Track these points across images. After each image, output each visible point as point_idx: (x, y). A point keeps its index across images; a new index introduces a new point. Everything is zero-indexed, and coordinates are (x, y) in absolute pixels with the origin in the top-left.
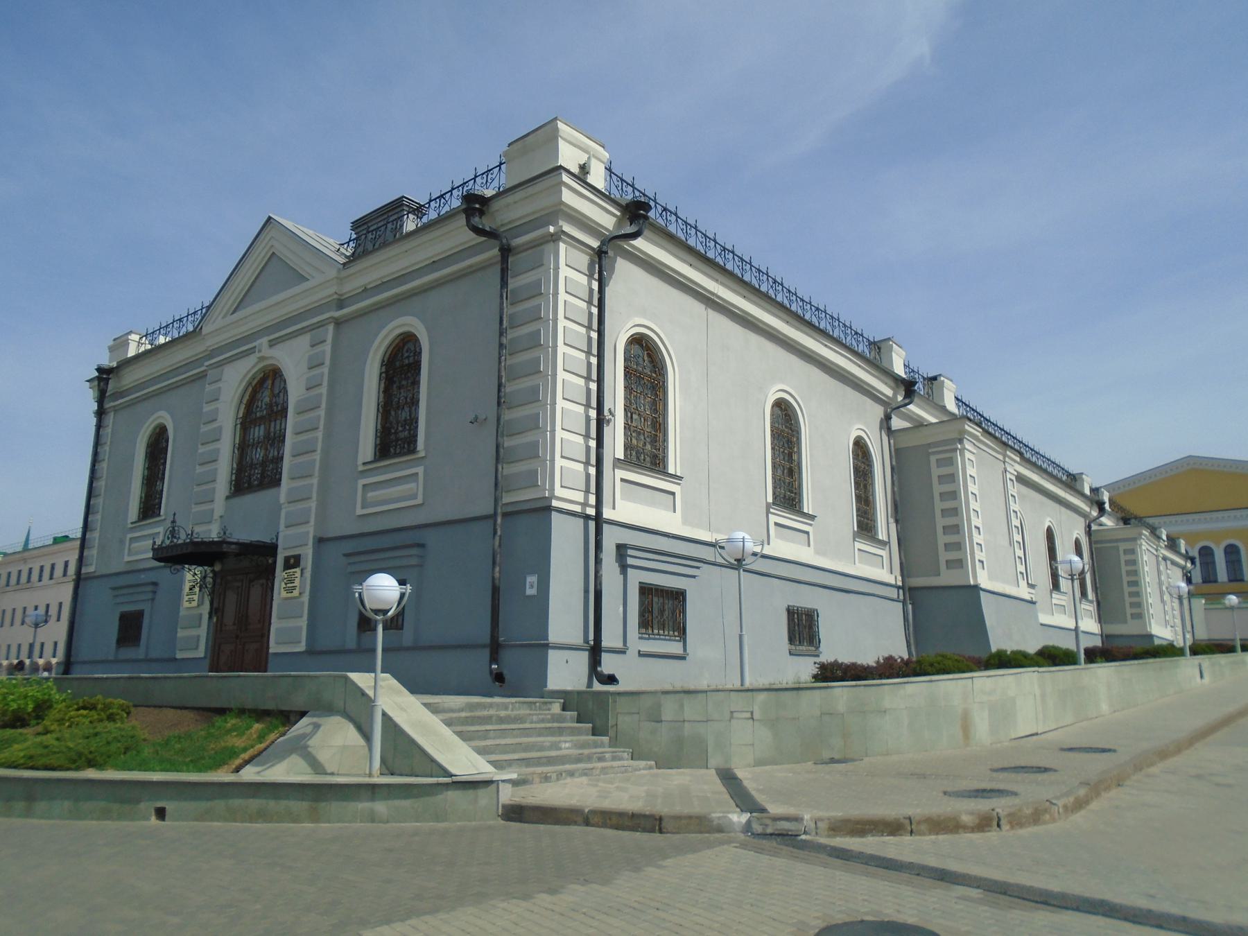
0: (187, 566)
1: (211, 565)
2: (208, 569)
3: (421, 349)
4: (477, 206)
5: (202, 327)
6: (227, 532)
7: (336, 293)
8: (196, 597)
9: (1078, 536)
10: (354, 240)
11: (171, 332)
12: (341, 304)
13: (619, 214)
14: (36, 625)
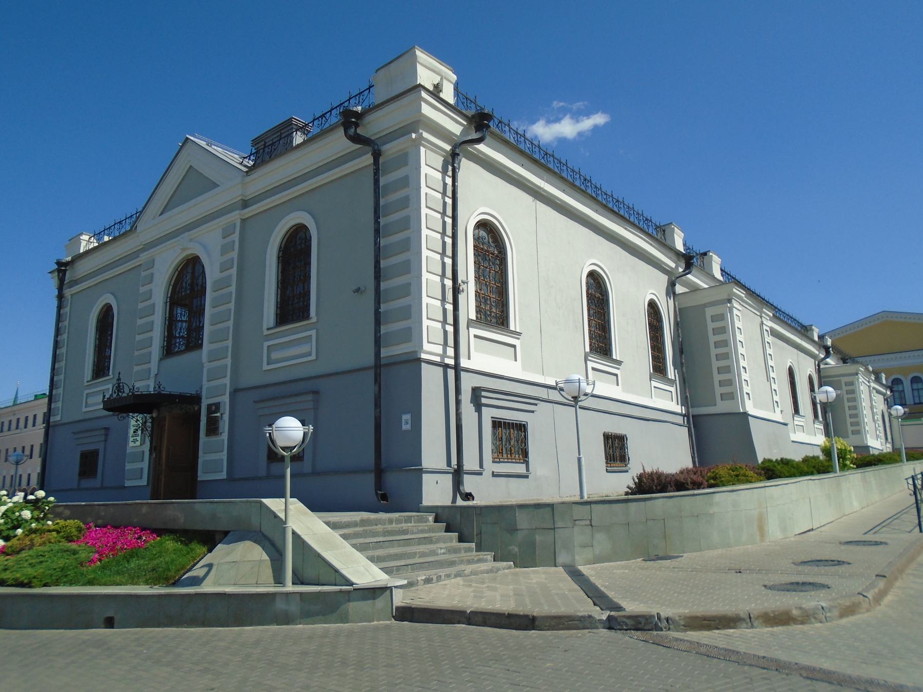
0: (131, 414)
1: (150, 412)
2: (148, 416)
3: (311, 237)
4: (353, 120)
6: (161, 387)
7: (241, 195)
8: (139, 438)
9: (810, 372)
10: (254, 154)
11: (113, 233)
12: (245, 204)
13: (465, 123)
14: (17, 463)
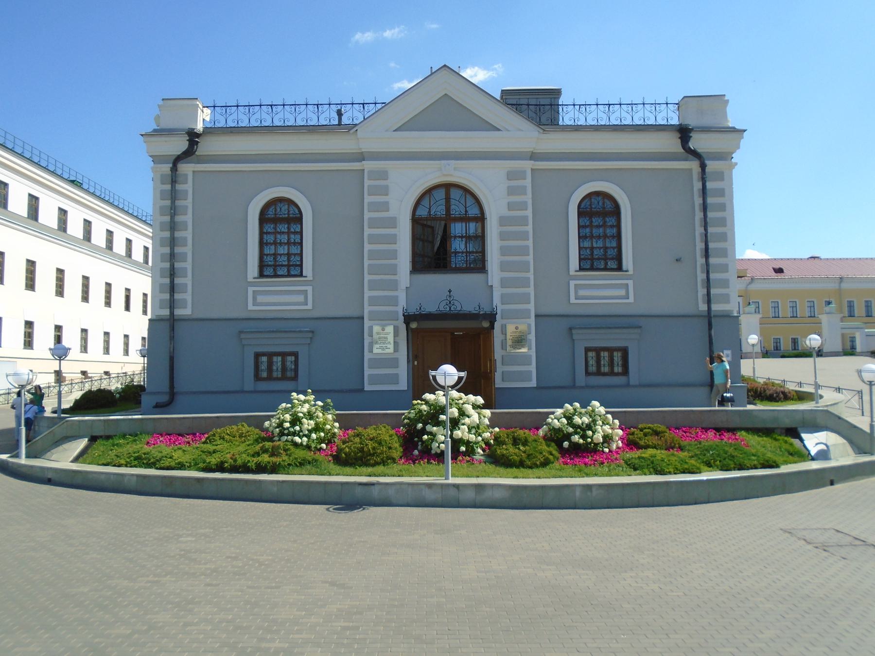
5: (357, 130)
8: (391, 346)
12: (534, 156)
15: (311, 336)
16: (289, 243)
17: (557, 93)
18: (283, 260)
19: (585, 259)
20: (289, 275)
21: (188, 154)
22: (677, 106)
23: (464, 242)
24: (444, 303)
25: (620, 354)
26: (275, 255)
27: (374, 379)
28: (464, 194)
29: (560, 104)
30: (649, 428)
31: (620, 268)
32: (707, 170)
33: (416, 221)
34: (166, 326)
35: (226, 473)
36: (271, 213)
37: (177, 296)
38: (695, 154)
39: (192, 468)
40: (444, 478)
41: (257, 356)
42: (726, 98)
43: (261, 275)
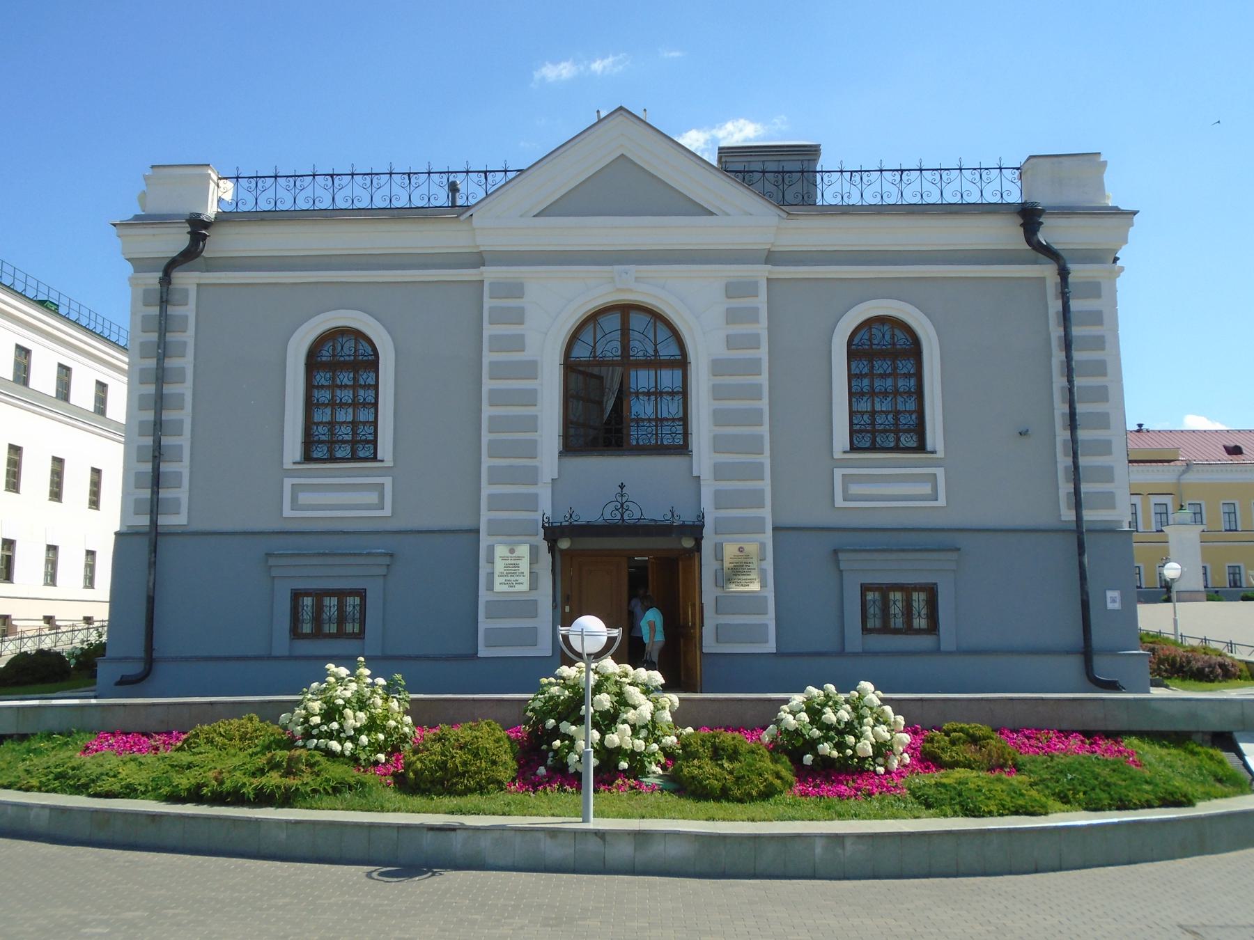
5: (472, 215)
8: (525, 580)
12: (771, 258)
15: (388, 563)
16: (355, 404)
17: (812, 152)
18: (345, 432)
19: (860, 431)
20: (354, 458)
21: (189, 256)
22: (1017, 172)
23: (652, 403)
24: (611, 507)
25: (923, 596)
26: (332, 424)
27: (497, 637)
28: (652, 321)
29: (817, 170)
30: (962, 730)
31: (921, 447)
32: (1071, 279)
33: (570, 366)
34: (144, 543)
35: (204, 804)
36: (326, 354)
37: (163, 493)
38: (1048, 252)
39: (148, 794)
40: (581, 820)
41: (297, 595)
42: (1102, 159)
43: (308, 457)
